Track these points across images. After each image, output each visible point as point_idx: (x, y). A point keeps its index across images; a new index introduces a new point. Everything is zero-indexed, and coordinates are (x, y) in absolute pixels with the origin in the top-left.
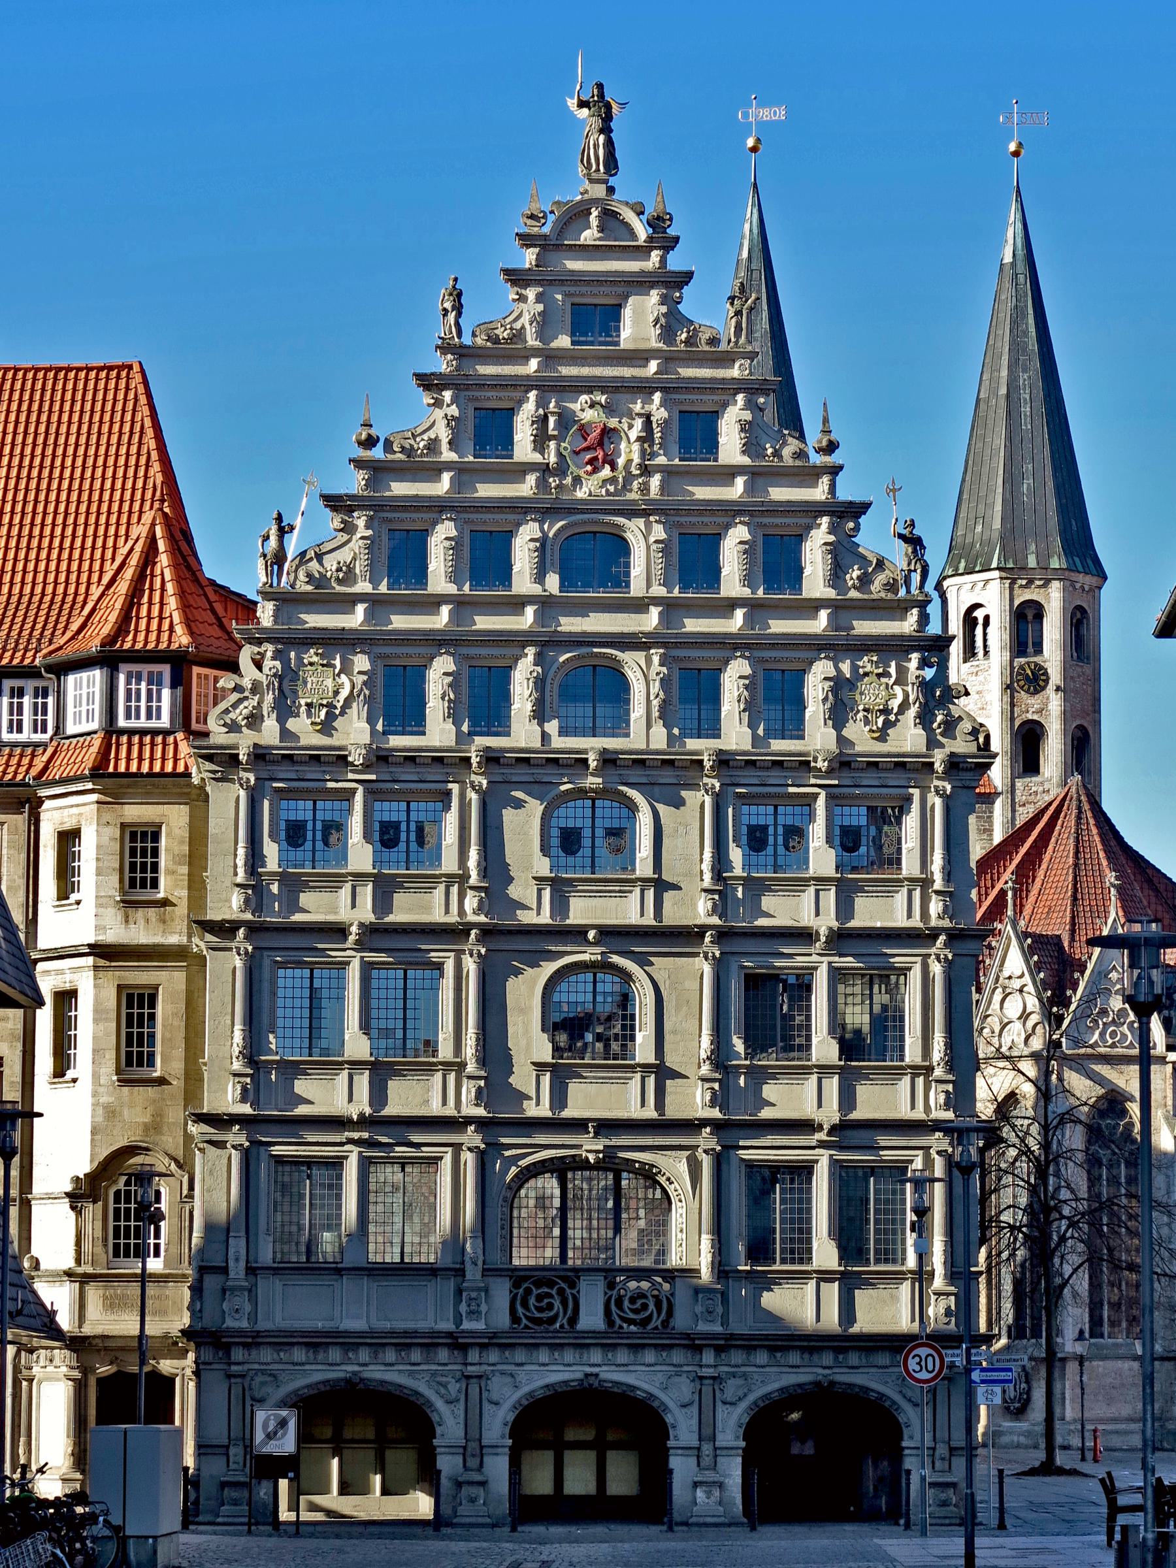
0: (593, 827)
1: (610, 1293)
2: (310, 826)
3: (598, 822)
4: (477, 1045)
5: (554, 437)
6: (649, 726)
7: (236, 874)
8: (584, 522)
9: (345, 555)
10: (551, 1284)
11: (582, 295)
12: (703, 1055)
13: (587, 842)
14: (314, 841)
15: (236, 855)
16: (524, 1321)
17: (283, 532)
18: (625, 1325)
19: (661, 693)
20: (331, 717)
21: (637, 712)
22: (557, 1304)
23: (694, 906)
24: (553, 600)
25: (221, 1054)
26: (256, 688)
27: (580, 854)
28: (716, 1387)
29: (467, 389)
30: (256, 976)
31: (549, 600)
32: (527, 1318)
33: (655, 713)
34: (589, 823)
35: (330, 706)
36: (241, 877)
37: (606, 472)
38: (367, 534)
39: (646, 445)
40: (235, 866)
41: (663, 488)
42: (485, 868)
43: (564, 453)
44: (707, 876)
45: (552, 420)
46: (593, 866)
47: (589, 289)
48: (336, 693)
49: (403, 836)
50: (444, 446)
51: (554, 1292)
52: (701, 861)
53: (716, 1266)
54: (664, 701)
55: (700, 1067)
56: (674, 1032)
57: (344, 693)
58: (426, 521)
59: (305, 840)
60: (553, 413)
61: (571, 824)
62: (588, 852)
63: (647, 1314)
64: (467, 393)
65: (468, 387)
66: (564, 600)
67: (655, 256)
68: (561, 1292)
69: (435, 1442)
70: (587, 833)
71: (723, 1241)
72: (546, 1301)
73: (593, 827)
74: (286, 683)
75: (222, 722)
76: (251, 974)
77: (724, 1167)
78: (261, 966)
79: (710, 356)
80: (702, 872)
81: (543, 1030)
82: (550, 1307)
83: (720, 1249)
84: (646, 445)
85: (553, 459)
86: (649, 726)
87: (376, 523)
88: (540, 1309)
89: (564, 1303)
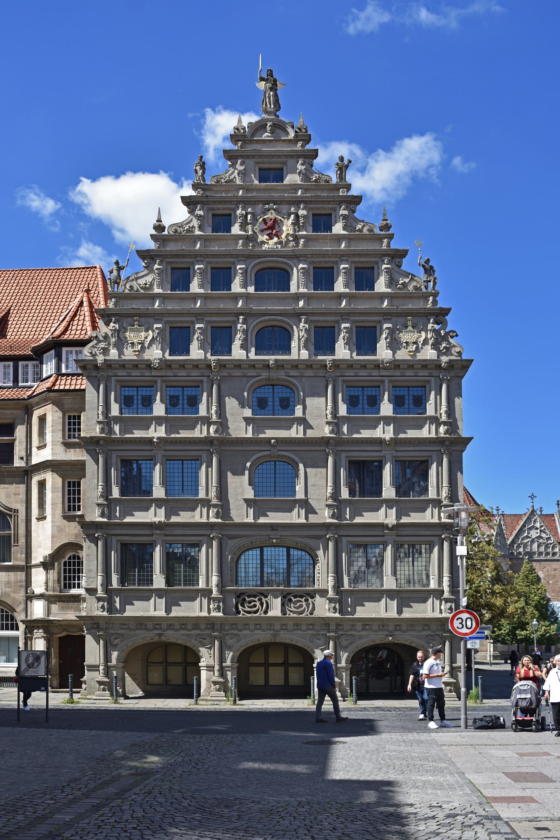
0: (273, 397)
1: (284, 600)
2: (135, 398)
3: (276, 395)
4: (216, 491)
5: (250, 224)
6: (299, 350)
7: (98, 417)
8: (266, 262)
9: (149, 278)
10: (255, 596)
11: (264, 163)
12: (329, 495)
13: (270, 403)
14: (137, 404)
15: (98, 409)
16: (242, 612)
17: (120, 269)
18: (291, 614)
19: (305, 335)
20: (143, 348)
21: (294, 344)
22: (258, 604)
23: (323, 430)
24: (251, 296)
25: (93, 496)
26: (106, 337)
27: (267, 408)
28: (337, 641)
29: (208, 204)
30: (109, 462)
31: (249, 296)
32: (244, 611)
33: (302, 344)
34: (271, 395)
35: (142, 343)
36: (101, 418)
37: (276, 239)
38: (159, 267)
39: (296, 227)
40: (98, 414)
41: (304, 245)
42: (220, 414)
43: (256, 231)
44: (329, 416)
45: (249, 217)
46: (274, 412)
47: (267, 160)
48: (146, 338)
49: (181, 402)
50: (197, 229)
51: (256, 600)
52: (326, 410)
53: (336, 588)
54: (307, 339)
55: (327, 500)
56: (314, 485)
57: (150, 338)
58: (189, 263)
59: (133, 404)
60: (250, 213)
61: (262, 395)
62: (271, 408)
63: (303, 608)
64: (208, 206)
65: (208, 203)
66: (257, 295)
67: (300, 144)
68: (260, 600)
69: (200, 664)
70: (270, 399)
71: (339, 577)
72: (253, 603)
73: (273, 397)
74: (121, 334)
75: (90, 351)
76: (106, 462)
77: (339, 545)
78: (111, 458)
79: (326, 187)
80: (327, 415)
81: (250, 485)
82: (255, 606)
83: (338, 580)
84: (296, 227)
85: (250, 233)
86: (299, 350)
87: (164, 264)
88: (250, 607)
89: (262, 604)
